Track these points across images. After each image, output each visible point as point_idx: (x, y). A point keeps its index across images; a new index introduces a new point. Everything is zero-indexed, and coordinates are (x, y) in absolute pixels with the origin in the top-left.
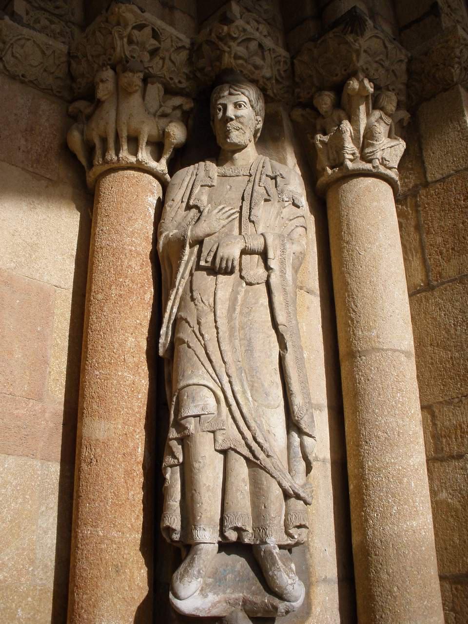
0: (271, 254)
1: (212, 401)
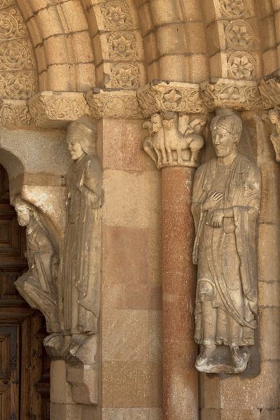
0: (236, 219)
1: (210, 288)
